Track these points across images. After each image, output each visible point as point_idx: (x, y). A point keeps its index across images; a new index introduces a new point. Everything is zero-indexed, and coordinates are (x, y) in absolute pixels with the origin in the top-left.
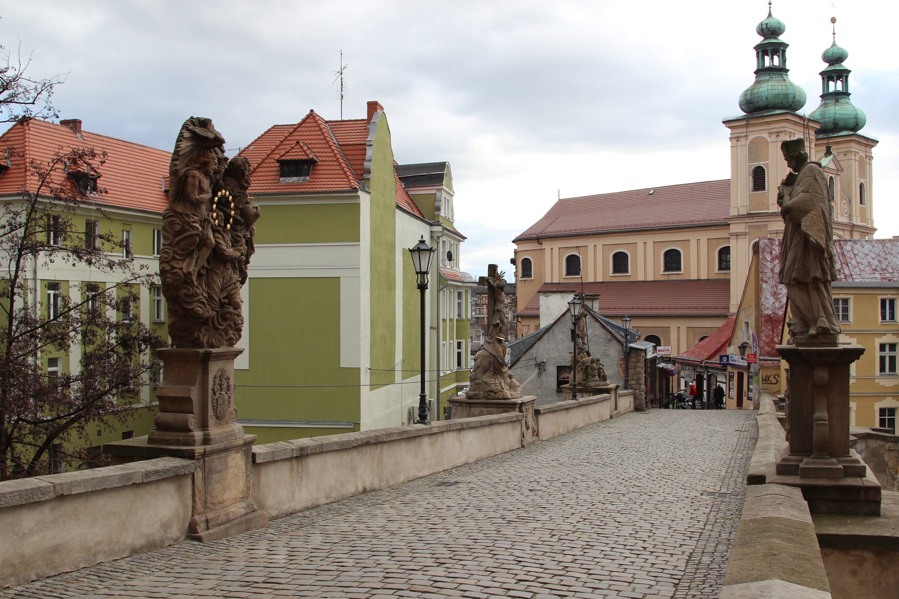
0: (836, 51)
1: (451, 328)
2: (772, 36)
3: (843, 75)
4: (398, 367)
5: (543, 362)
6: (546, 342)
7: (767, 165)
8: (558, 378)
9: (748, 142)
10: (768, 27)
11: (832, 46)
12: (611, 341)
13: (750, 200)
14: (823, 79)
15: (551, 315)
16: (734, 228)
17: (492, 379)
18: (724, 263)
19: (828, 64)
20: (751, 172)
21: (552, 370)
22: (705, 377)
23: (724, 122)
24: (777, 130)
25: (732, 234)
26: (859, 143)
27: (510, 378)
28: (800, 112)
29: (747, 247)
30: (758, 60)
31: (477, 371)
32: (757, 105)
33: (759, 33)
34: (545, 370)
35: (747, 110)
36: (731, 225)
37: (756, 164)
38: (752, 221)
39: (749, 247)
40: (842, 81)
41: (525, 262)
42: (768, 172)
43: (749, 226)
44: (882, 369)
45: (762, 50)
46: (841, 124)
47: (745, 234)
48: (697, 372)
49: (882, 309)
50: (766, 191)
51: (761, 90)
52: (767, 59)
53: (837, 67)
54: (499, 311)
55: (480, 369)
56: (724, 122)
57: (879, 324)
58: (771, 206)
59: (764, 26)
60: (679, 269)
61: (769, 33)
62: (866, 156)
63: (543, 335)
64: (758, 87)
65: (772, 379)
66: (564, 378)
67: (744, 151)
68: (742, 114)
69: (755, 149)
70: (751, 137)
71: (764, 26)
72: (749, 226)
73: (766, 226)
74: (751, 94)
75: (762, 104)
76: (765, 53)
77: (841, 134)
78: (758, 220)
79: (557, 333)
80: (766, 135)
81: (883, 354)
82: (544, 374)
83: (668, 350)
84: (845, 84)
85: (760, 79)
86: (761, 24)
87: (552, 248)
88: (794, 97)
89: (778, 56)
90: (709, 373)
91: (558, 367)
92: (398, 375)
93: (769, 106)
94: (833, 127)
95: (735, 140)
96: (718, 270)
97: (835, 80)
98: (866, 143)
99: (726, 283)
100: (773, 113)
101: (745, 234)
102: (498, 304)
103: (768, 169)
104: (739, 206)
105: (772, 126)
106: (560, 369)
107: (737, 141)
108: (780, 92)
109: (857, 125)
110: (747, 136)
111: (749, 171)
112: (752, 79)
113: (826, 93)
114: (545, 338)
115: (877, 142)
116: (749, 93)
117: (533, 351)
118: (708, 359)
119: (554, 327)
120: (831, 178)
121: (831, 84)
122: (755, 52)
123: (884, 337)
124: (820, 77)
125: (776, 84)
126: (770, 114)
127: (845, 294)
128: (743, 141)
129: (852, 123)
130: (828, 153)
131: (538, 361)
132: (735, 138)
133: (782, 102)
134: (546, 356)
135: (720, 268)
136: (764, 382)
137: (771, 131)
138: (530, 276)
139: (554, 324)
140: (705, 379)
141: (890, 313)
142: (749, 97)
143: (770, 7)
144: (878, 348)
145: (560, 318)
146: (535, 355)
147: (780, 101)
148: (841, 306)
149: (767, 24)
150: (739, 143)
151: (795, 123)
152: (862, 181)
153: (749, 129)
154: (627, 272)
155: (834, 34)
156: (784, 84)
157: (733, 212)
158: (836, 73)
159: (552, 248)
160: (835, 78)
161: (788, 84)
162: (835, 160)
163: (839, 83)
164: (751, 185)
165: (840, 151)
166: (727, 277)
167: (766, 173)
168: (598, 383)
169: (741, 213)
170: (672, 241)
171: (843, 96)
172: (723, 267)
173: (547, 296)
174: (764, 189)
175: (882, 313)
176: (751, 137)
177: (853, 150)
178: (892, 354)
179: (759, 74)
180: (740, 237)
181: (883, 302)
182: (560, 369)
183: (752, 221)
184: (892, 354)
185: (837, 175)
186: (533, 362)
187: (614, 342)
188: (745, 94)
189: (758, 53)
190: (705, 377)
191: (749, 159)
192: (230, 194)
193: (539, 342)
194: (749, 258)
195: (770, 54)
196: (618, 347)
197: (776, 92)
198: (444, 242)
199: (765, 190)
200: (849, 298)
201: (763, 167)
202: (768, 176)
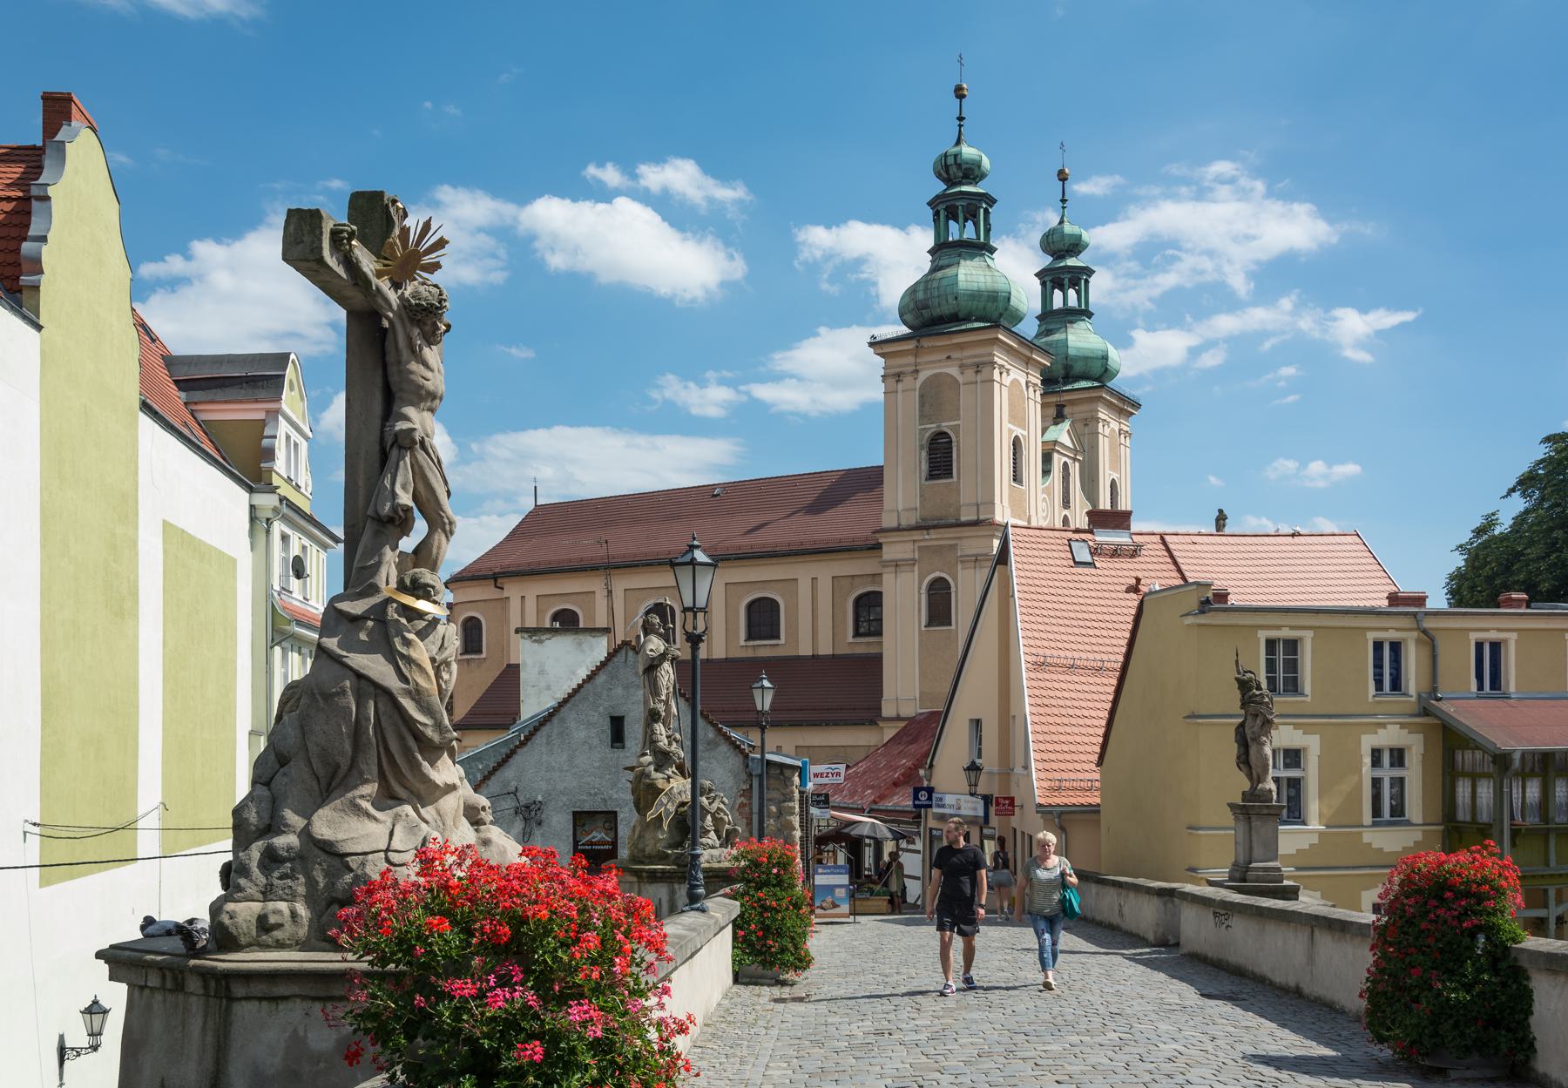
0: (1068, 229)
2: (964, 181)
3: (1079, 277)
4: (153, 821)
6: (544, 749)
7: (956, 429)
8: (576, 843)
9: (918, 387)
10: (959, 161)
11: (1061, 222)
12: (717, 745)
13: (921, 496)
14: (1043, 284)
15: (548, 688)
16: (889, 552)
17: (371, 826)
18: (865, 624)
19: (1050, 259)
20: (924, 442)
21: (559, 822)
23: (874, 344)
24: (976, 360)
25: (885, 564)
26: (1110, 405)
27: (476, 823)
28: (1018, 329)
29: (916, 590)
30: (936, 227)
31: (280, 780)
32: (937, 312)
33: (939, 175)
34: (540, 823)
35: (916, 323)
36: (885, 548)
37: (933, 427)
38: (927, 537)
39: (920, 588)
40: (1078, 293)
41: (469, 624)
42: (958, 442)
43: (920, 547)
44: (1377, 811)
45: (946, 209)
46: (1078, 368)
47: (913, 562)
49: (1375, 666)
50: (955, 479)
51: (944, 282)
52: (953, 226)
53: (1071, 262)
54: (409, 443)
55: (297, 768)
56: (871, 345)
57: (1370, 699)
58: (963, 511)
59: (951, 161)
60: (778, 637)
61: (961, 174)
62: (1120, 430)
63: (536, 729)
64: (939, 274)
66: (592, 844)
67: (910, 402)
68: (905, 330)
69: (934, 398)
70: (924, 375)
71: (951, 161)
72: (920, 547)
73: (954, 547)
74: (926, 290)
75: (946, 310)
76: (952, 214)
77: (1077, 386)
78: (938, 536)
79: (573, 725)
80: (953, 371)
81: (1378, 773)
82: (537, 832)
83: (838, 774)
84: (1083, 295)
85: (941, 263)
86: (946, 155)
87: (523, 597)
88: (1009, 299)
89: (976, 225)
91: (575, 813)
92: (148, 842)
93: (961, 315)
94: (1062, 372)
95: (892, 381)
96: (854, 637)
97: (1066, 287)
98: (1121, 405)
99: (874, 663)
100: (970, 326)
101: (913, 562)
102: (410, 411)
103: (957, 437)
104: (900, 508)
105: (967, 353)
106: (581, 819)
107: (897, 381)
108: (982, 287)
109: (1106, 370)
110: (917, 371)
111: (921, 440)
112: (926, 263)
113: (1048, 309)
114: (540, 739)
115: (1137, 406)
116: (921, 287)
117: (509, 773)
118: (875, 802)
119: (564, 710)
120: (1065, 463)
121: (1058, 294)
122: (930, 212)
123: (1381, 731)
124: (1037, 282)
125: (974, 272)
126: (963, 327)
127: (1292, 628)
128: (908, 381)
129: (1096, 369)
130: (1059, 418)
131: (521, 798)
132: (893, 377)
133: (984, 308)
134: (543, 785)
135: (857, 634)
137: (964, 361)
138: (480, 652)
139: (565, 701)
140: (870, 845)
141: (1391, 674)
142: (920, 295)
143: (960, 126)
144: (1367, 760)
145: (580, 686)
146: (514, 784)
147: (981, 305)
148: (1281, 657)
149: (956, 156)
150: (900, 386)
151: (1009, 350)
152: (1115, 476)
153: (918, 360)
155: (1063, 201)
156: (988, 273)
157: (888, 521)
158: (1070, 272)
159: (523, 597)
160: (1066, 282)
161: (996, 274)
162: (1075, 433)
163: (1072, 293)
164: (925, 466)
165: (1077, 416)
166: (873, 650)
167: (954, 444)
168: (715, 852)
169: (904, 523)
170: (761, 577)
171: (1078, 317)
172: (862, 630)
173: (540, 642)
174: (949, 474)
175: (1375, 675)
176: (924, 375)
177: (1101, 415)
178: (1397, 773)
179: (937, 255)
180: (903, 568)
181: (1378, 646)
182: (581, 819)
183: (927, 537)
184: (1397, 773)
185: (1075, 459)
186: (508, 804)
187: (724, 748)
188: (913, 290)
189: (937, 214)
191: (924, 417)
193: (525, 749)
194: (920, 610)
195: (961, 220)
196: (735, 761)
197: (975, 287)
198: (285, 538)
199: (952, 477)
200: (1301, 639)
202: (958, 450)
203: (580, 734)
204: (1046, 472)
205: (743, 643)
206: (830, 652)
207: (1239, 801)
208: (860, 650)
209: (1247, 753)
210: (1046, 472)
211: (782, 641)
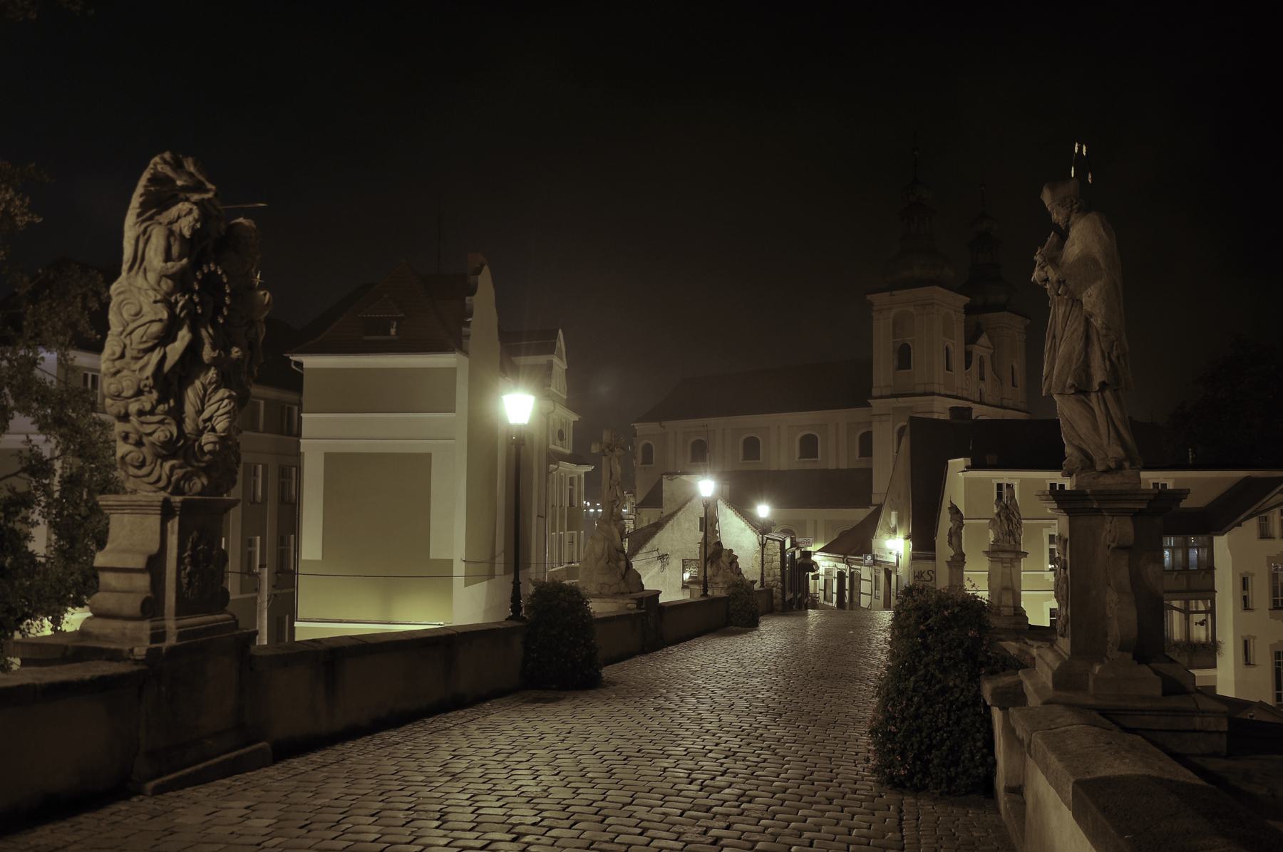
1: (562, 517)
5: (666, 555)
22: (847, 574)
39: (893, 432)
48: (838, 568)
65: (925, 575)
82: (667, 568)
90: (852, 570)
96: (859, 457)
99: (868, 472)
135: (861, 455)
136: (917, 579)
146: (657, 547)
154: (759, 459)
167: (912, 351)
174: (910, 368)
190: (847, 574)
192: (224, 272)
201: (910, 344)
203: (686, 525)
204: (968, 366)
205: (797, 459)
206: (845, 467)
207: (950, 559)
208: (863, 465)
209: (951, 540)
210: (968, 364)
211: (819, 459)
